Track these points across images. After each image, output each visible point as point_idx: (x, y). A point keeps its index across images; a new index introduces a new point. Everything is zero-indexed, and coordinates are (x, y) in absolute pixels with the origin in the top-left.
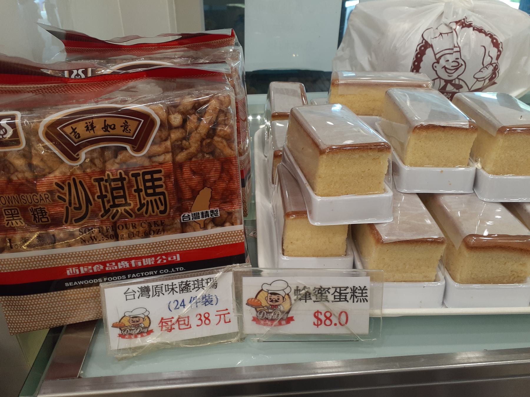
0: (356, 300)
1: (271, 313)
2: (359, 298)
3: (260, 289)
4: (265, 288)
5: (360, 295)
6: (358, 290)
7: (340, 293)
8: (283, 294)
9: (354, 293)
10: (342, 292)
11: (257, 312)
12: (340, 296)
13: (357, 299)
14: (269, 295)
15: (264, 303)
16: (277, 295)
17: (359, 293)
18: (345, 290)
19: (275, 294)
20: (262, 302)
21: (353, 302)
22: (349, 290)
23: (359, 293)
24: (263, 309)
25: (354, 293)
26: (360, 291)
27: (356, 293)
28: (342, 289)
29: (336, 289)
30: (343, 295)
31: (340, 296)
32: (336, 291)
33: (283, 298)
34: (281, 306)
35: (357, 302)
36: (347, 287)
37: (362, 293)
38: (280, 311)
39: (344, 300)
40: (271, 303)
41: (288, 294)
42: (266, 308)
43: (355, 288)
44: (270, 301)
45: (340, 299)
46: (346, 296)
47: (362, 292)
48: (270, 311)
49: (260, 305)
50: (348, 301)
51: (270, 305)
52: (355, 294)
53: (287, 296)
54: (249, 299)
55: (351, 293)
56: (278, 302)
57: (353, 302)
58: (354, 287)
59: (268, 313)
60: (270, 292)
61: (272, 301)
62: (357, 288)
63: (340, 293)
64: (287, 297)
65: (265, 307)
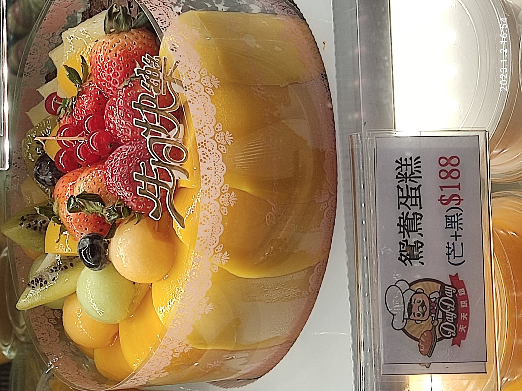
0: (417, 174)
4: (399, 323)
5: (409, 167)
6: (402, 171)
7: (408, 197)
9: (406, 178)
11: (443, 338)
13: (415, 172)
14: (412, 317)
15: (427, 325)
16: (412, 303)
17: (407, 170)
18: (402, 190)
21: (421, 177)
22: (403, 185)
23: (407, 170)
24: (437, 327)
26: (404, 168)
27: (406, 174)
29: (401, 203)
31: (412, 197)
32: (404, 204)
33: (416, 292)
34: (431, 297)
35: (420, 172)
37: (407, 165)
38: (440, 298)
39: (417, 192)
41: (410, 285)
42: (436, 321)
43: (399, 176)
44: (423, 316)
45: (416, 197)
46: (411, 189)
47: (404, 165)
48: (440, 316)
50: (420, 186)
51: (430, 315)
52: (408, 176)
55: (406, 182)
56: (423, 301)
57: (421, 177)
58: (397, 177)
62: (399, 173)
63: (408, 197)
64: (415, 287)
65: (435, 324)
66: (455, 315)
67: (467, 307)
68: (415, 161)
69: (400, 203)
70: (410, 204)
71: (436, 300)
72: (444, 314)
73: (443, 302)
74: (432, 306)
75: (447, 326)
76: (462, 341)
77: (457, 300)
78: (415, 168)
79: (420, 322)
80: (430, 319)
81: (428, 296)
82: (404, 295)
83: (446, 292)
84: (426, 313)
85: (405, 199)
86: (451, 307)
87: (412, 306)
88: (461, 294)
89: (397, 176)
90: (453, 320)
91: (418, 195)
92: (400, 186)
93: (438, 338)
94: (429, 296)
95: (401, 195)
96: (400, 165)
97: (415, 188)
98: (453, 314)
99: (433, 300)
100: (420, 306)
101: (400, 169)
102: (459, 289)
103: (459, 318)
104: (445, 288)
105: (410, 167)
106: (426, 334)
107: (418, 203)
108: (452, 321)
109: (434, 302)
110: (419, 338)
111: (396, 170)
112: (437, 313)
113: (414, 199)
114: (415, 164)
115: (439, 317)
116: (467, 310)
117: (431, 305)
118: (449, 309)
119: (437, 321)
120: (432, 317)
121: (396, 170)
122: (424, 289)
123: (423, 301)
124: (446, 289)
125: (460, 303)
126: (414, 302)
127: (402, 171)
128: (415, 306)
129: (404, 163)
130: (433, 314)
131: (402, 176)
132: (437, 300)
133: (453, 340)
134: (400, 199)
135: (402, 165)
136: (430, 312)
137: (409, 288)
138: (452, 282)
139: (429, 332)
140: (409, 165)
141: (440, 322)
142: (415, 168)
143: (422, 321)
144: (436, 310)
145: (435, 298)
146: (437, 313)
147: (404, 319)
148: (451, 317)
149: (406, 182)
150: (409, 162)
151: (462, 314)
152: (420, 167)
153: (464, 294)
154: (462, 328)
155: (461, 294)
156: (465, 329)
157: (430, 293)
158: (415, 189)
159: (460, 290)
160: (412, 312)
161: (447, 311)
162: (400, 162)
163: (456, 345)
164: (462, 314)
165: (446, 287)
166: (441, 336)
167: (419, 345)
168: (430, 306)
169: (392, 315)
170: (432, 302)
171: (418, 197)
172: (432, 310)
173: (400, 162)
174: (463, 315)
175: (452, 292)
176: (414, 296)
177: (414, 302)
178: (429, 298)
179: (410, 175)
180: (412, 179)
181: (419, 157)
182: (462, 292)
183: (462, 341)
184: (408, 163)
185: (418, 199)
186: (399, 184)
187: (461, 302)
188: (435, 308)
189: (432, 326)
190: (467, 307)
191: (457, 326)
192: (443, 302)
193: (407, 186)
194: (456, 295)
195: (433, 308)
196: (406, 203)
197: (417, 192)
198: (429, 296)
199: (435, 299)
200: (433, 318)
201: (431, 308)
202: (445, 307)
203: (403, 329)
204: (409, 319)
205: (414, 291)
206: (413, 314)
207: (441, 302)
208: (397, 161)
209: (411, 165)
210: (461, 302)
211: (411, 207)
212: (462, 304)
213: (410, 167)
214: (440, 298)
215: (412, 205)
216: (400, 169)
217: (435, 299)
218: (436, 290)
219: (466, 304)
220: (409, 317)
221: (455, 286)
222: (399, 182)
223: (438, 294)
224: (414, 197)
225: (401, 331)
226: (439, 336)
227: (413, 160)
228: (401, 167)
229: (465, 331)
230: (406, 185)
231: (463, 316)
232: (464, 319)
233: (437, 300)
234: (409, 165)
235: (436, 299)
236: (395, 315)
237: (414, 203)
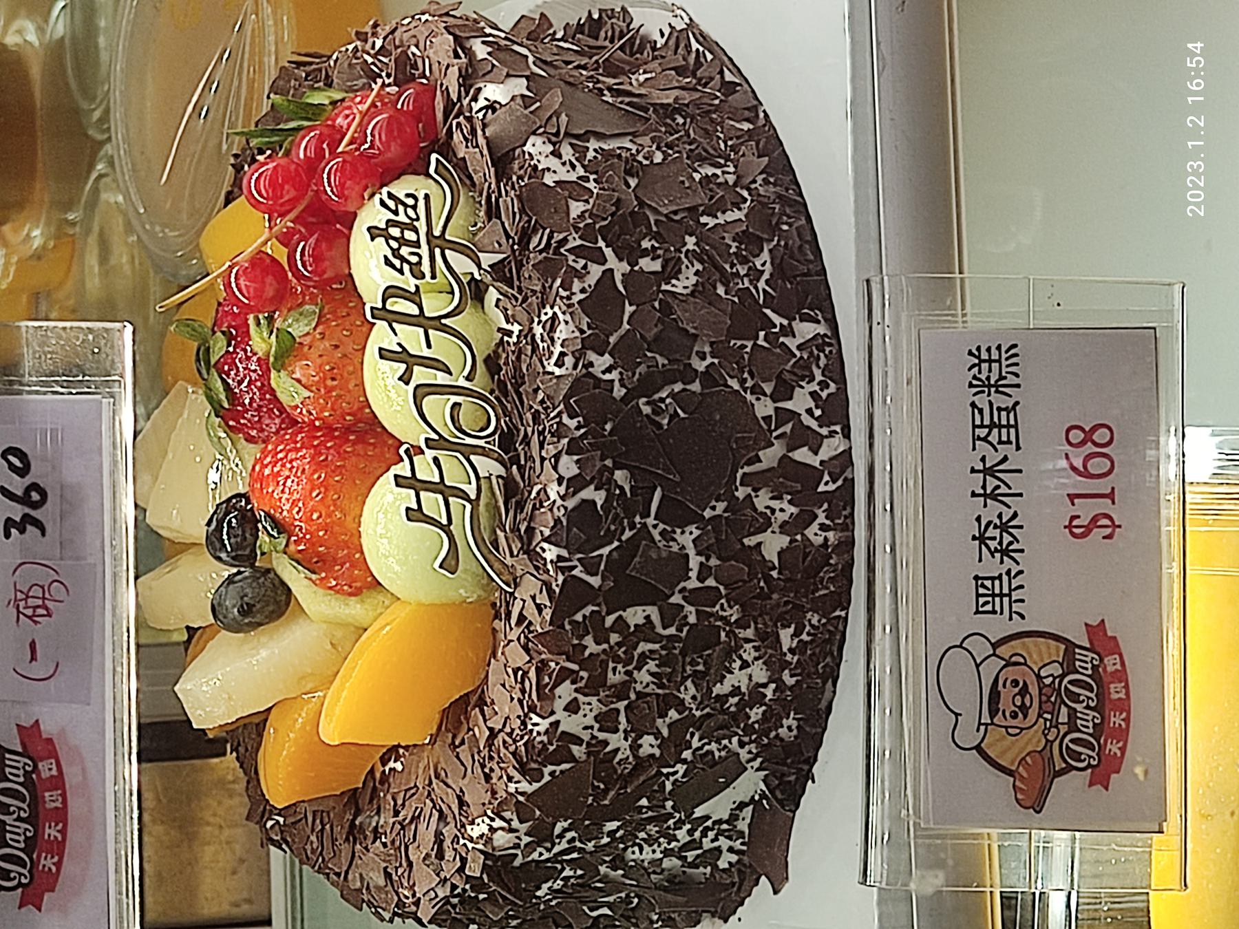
0: (1011, 380)
1: (1072, 713)
2: (1004, 370)
3: (974, 751)
5: (995, 366)
6: (980, 372)
8: (996, 664)
9: (990, 386)
10: (987, 422)
11: (1071, 768)
12: (1000, 427)
13: (1008, 375)
15: (1033, 740)
17: (990, 371)
18: (981, 411)
19: (995, 695)
20: (1030, 748)
21: (1018, 386)
23: (990, 371)
25: (990, 386)
26: (985, 366)
27: (988, 378)
28: (978, 422)
30: (996, 419)
34: (1043, 674)
35: (1017, 375)
36: (973, 405)
38: (1062, 676)
40: (1033, 713)
41: (995, 646)
43: (975, 382)
44: (1025, 717)
46: (999, 409)
47: (985, 361)
48: (1063, 718)
49: (1044, 754)
50: (1017, 403)
51: (1040, 716)
52: (992, 382)
54: (1017, 799)
55: (989, 395)
56: (1025, 683)
57: (1018, 386)
58: (971, 385)
59: (1073, 728)
60: (986, 719)
61: (1024, 709)
62: (975, 377)
66: (1098, 716)
67: (1124, 697)
68: (1007, 352)
69: (976, 438)
70: (997, 439)
71: (1053, 682)
73: (1070, 687)
74: (1045, 695)
75: (1079, 742)
76: (1114, 776)
78: (1008, 366)
79: (1018, 731)
80: (1040, 727)
82: (980, 668)
84: (1030, 711)
85: (987, 430)
86: (1089, 698)
87: (999, 693)
88: (1110, 669)
89: (970, 383)
90: (1093, 727)
91: (1012, 422)
92: (977, 403)
93: (1057, 769)
94: (1039, 670)
95: (978, 422)
96: (977, 361)
97: (1008, 407)
98: (1093, 713)
99: (1048, 681)
100: (1019, 693)
101: (977, 368)
102: (1107, 656)
103: (1106, 721)
105: (997, 364)
106: (1031, 758)
107: (1013, 438)
108: (1091, 731)
109: (1049, 686)
110: (1014, 768)
111: (970, 369)
112: (1056, 713)
113: (1004, 431)
114: (1007, 359)
115: (1060, 721)
116: (1124, 706)
117: (1044, 691)
119: (1056, 730)
120: (1046, 720)
121: (970, 369)
122: (1025, 655)
123: (1025, 683)
124: (1078, 657)
125: (1109, 688)
126: (1004, 686)
127: (980, 372)
128: (1007, 693)
129: (984, 356)
130: (1048, 713)
131: (980, 383)
132: (1057, 681)
133: (1092, 772)
134: (977, 430)
135: (982, 361)
136: (1040, 708)
137: (991, 652)
138: (1091, 643)
139: (1037, 754)
140: (995, 361)
141: (1061, 734)
142: (1008, 366)
143: (1022, 729)
144: (1054, 704)
145: (1052, 675)
146: (1056, 713)
147: (980, 724)
149: (989, 395)
150: (995, 356)
151: (1112, 713)
152: (1017, 364)
153: (1118, 667)
154: (1113, 748)
155: (1110, 669)
156: (1119, 748)
157: (1042, 664)
158: (1006, 409)
159: (1109, 658)
160: (999, 709)
161: (1079, 707)
162: (977, 353)
163: (1099, 787)
164: (1112, 713)
165: (1077, 650)
166: (1064, 765)
167: (1014, 786)
168: (1040, 694)
169: (953, 716)
171: (1012, 426)
172: (1046, 702)
173: (977, 353)
174: (1115, 716)
175: (1091, 662)
177: (1004, 686)
178: (1038, 676)
179: (997, 381)
180: (1000, 389)
181: (1015, 346)
182: (1114, 664)
183: (1114, 776)
184: (993, 358)
185: (1012, 431)
186: (976, 399)
187: (1112, 686)
188: (1053, 699)
189: (1044, 741)
190: (1124, 697)
191: (1102, 741)
192: (1070, 687)
193: (991, 404)
194: (1100, 670)
195: (1049, 700)
196: (989, 439)
197: (1012, 415)
198: (1039, 670)
199: (1051, 679)
200: (1048, 723)
201: (1044, 698)
202: (1075, 698)
203: (978, 748)
204: (992, 723)
205: (1003, 659)
206: (1000, 713)
207: (1066, 686)
208: (970, 353)
209: (999, 361)
210: (1112, 686)
211: (998, 447)
212: (1112, 690)
213: (997, 364)
214: (1062, 676)
215: (1000, 442)
216: (977, 368)
217: (1051, 679)
218: (1055, 658)
219: (1124, 690)
220: (992, 719)
221: (1098, 649)
222: (975, 395)
224: (1004, 426)
225: (974, 751)
226: (1060, 765)
227: (1003, 349)
228: (979, 365)
229: (1119, 754)
230: (990, 401)
231: (1116, 720)
232: (1117, 725)
234: (995, 361)
235: (1055, 678)
236: (960, 715)
237: (1004, 438)
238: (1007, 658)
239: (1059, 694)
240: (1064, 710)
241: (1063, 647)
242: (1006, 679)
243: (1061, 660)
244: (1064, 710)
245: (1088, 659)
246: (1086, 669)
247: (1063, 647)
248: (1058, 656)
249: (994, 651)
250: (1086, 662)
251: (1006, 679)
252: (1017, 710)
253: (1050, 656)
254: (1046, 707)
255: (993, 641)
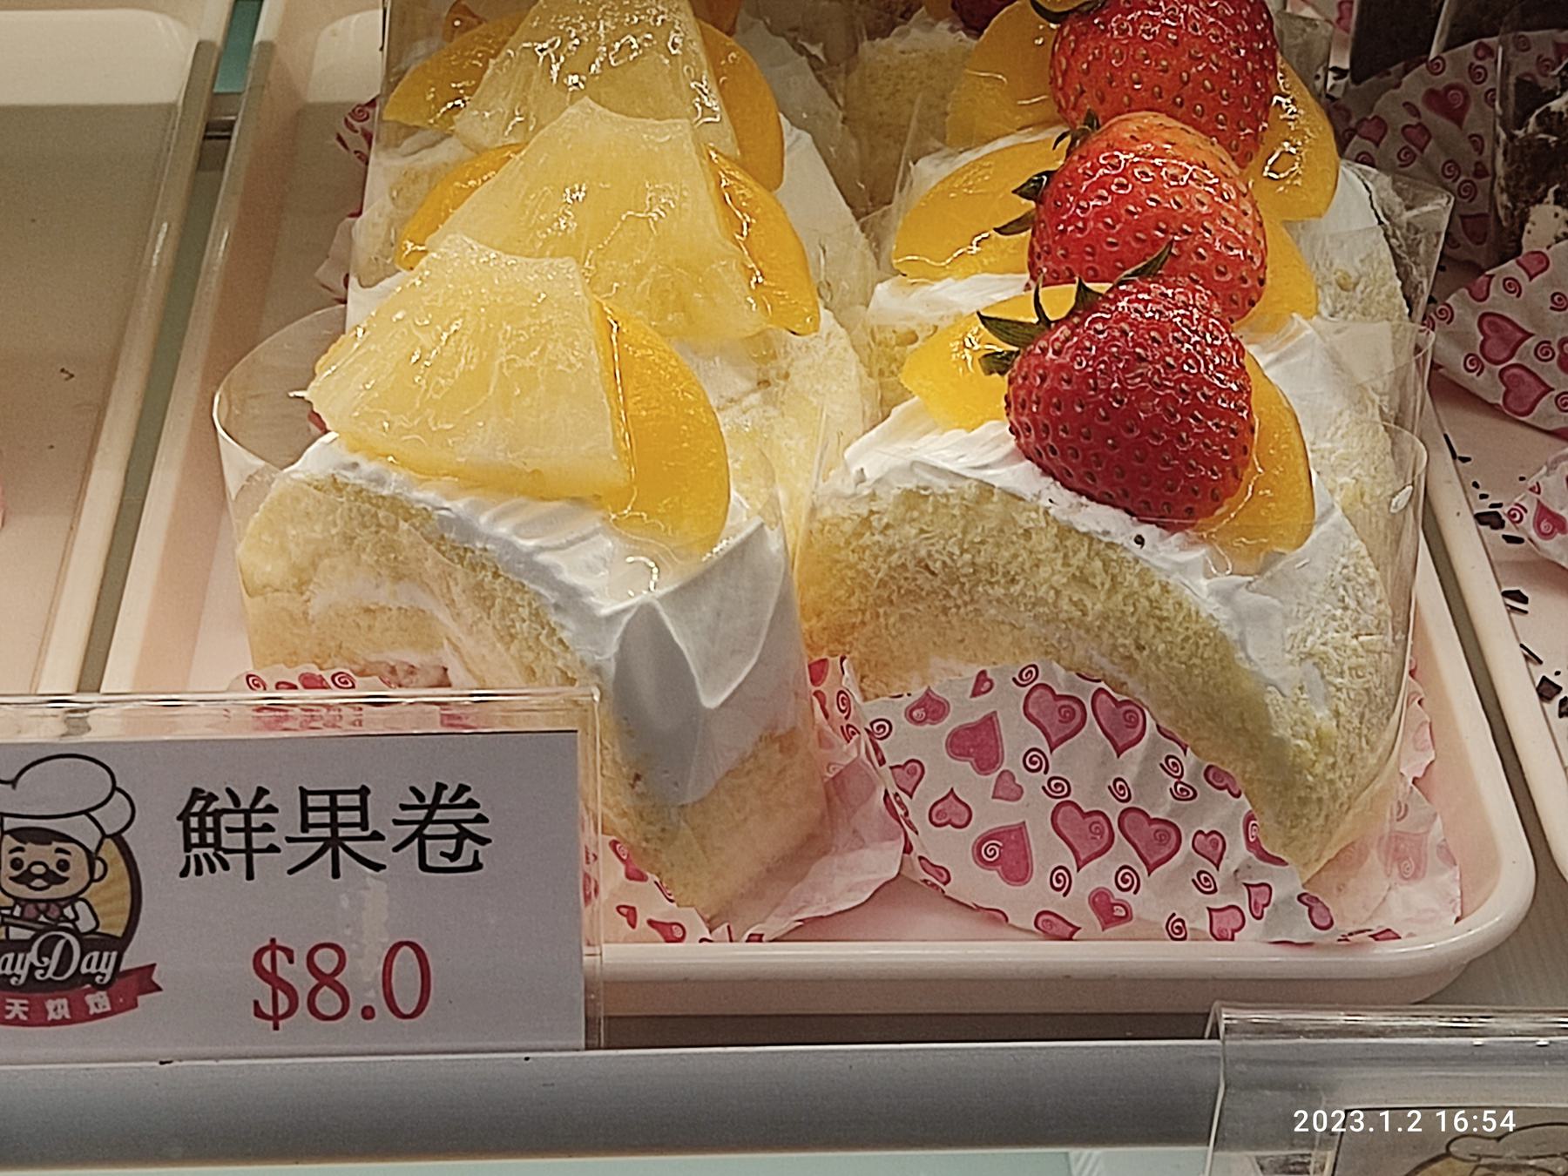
1: (24, 946)
8: (91, 839)
33: (92, 857)
34: (80, 905)
38: (75, 932)
40: (22, 891)
41: (117, 837)
44: (12, 879)
51: (17, 900)
53: (108, 842)
56: (66, 879)
61: (25, 878)
64: (110, 851)
71: (67, 920)
72: (26, 946)
73: (60, 944)
74: (48, 908)
77: (72, 987)
81: (82, 896)
83: (96, 954)
86: (46, 969)
99: (68, 912)
104: (111, 950)
109: (62, 914)
115: (11, 928)
118: (42, 962)
120: (12, 909)
123: (66, 879)
124: (106, 954)
126: (59, 850)
130: (22, 912)
132: (70, 925)
137: (108, 831)
138: (128, 972)
144: (35, 920)
145: (77, 918)
148: (13, 967)
157: (92, 902)
161: (32, 957)
165: (114, 954)
168: (48, 901)
170: (62, 908)
172: (37, 909)
175: (99, 973)
176: (80, 849)
177: (59, 850)
178: (73, 899)
188: (42, 919)
192: (60, 944)
195: (41, 912)
199: (72, 916)
201: (42, 906)
202: (45, 951)
207: (62, 937)
214: (75, 932)
217: (72, 916)
223: (89, 928)
233: (70, 925)
235: (73, 922)
238: (101, 854)
239: (49, 928)
240: (27, 934)
241: (119, 933)
242: (68, 853)
243: (99, 930)
244: (27, 934)
245: (102, 969)
246: (89, 966)
247: (119, 933)
248: (104, 927)
249: (112, 836)
250: (98, 966)
251: (68, 853)
252: (25, 867)
253: (104, 914)
254: (31, 911)
255: (124, 834)
